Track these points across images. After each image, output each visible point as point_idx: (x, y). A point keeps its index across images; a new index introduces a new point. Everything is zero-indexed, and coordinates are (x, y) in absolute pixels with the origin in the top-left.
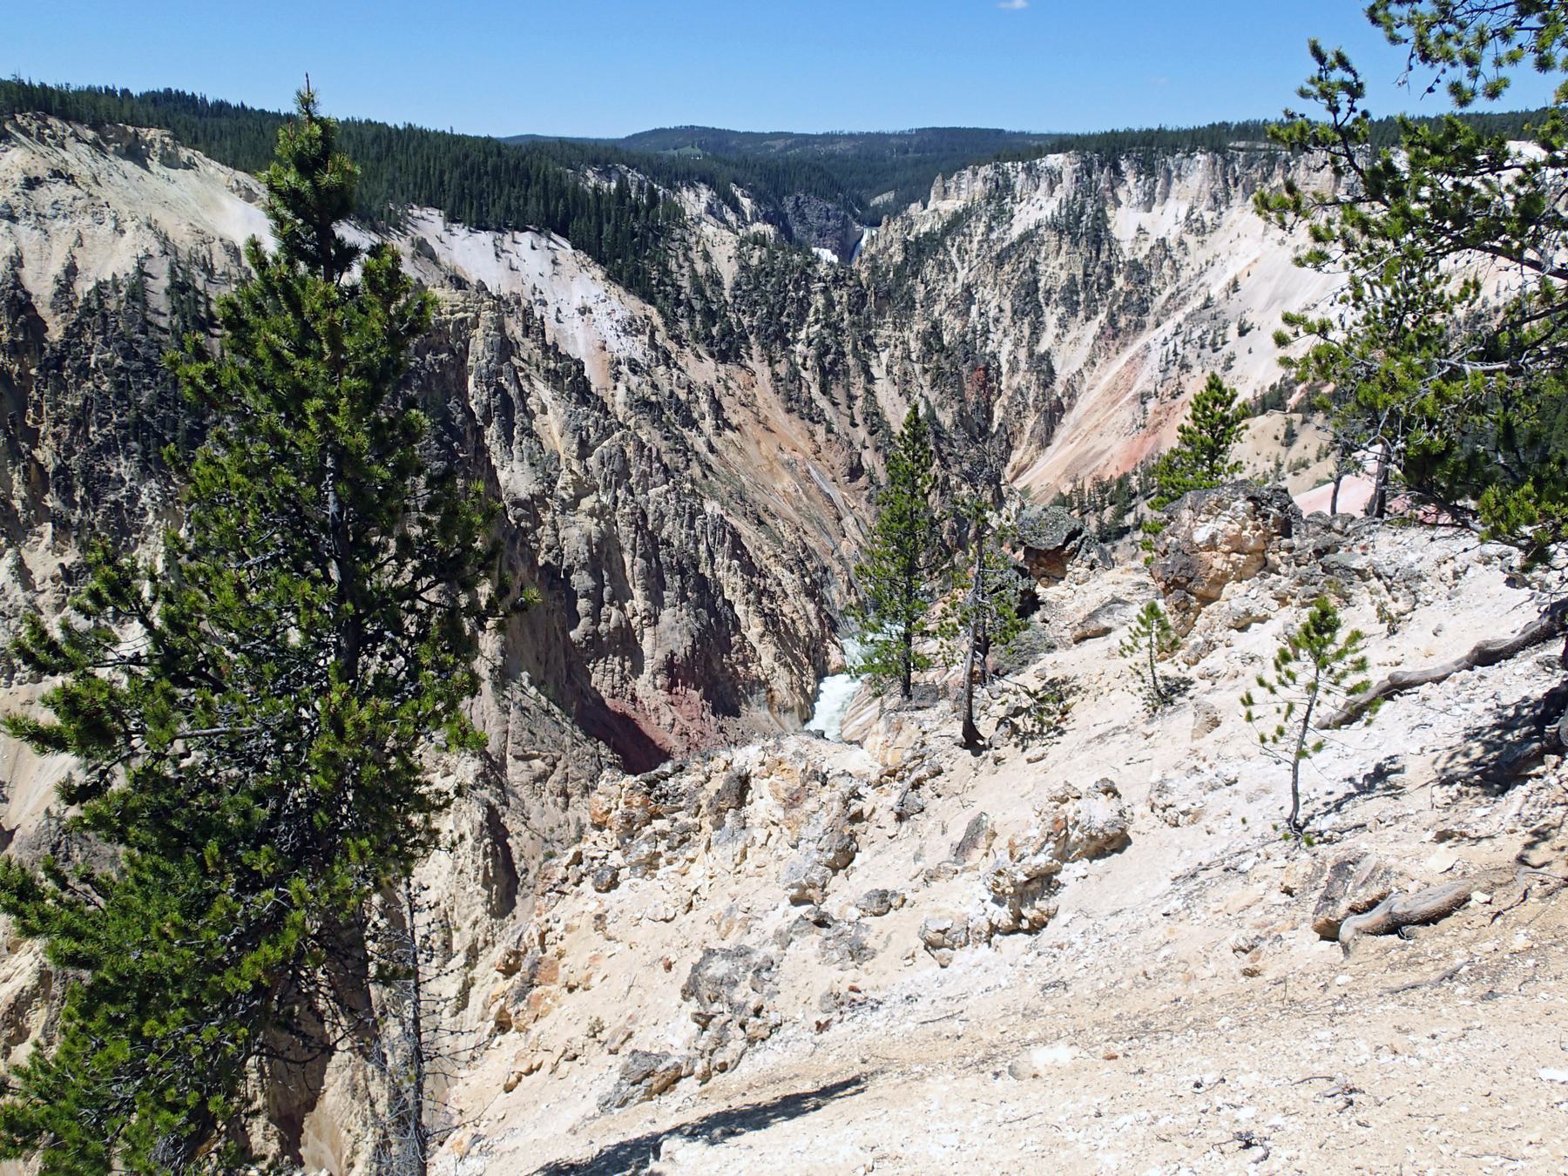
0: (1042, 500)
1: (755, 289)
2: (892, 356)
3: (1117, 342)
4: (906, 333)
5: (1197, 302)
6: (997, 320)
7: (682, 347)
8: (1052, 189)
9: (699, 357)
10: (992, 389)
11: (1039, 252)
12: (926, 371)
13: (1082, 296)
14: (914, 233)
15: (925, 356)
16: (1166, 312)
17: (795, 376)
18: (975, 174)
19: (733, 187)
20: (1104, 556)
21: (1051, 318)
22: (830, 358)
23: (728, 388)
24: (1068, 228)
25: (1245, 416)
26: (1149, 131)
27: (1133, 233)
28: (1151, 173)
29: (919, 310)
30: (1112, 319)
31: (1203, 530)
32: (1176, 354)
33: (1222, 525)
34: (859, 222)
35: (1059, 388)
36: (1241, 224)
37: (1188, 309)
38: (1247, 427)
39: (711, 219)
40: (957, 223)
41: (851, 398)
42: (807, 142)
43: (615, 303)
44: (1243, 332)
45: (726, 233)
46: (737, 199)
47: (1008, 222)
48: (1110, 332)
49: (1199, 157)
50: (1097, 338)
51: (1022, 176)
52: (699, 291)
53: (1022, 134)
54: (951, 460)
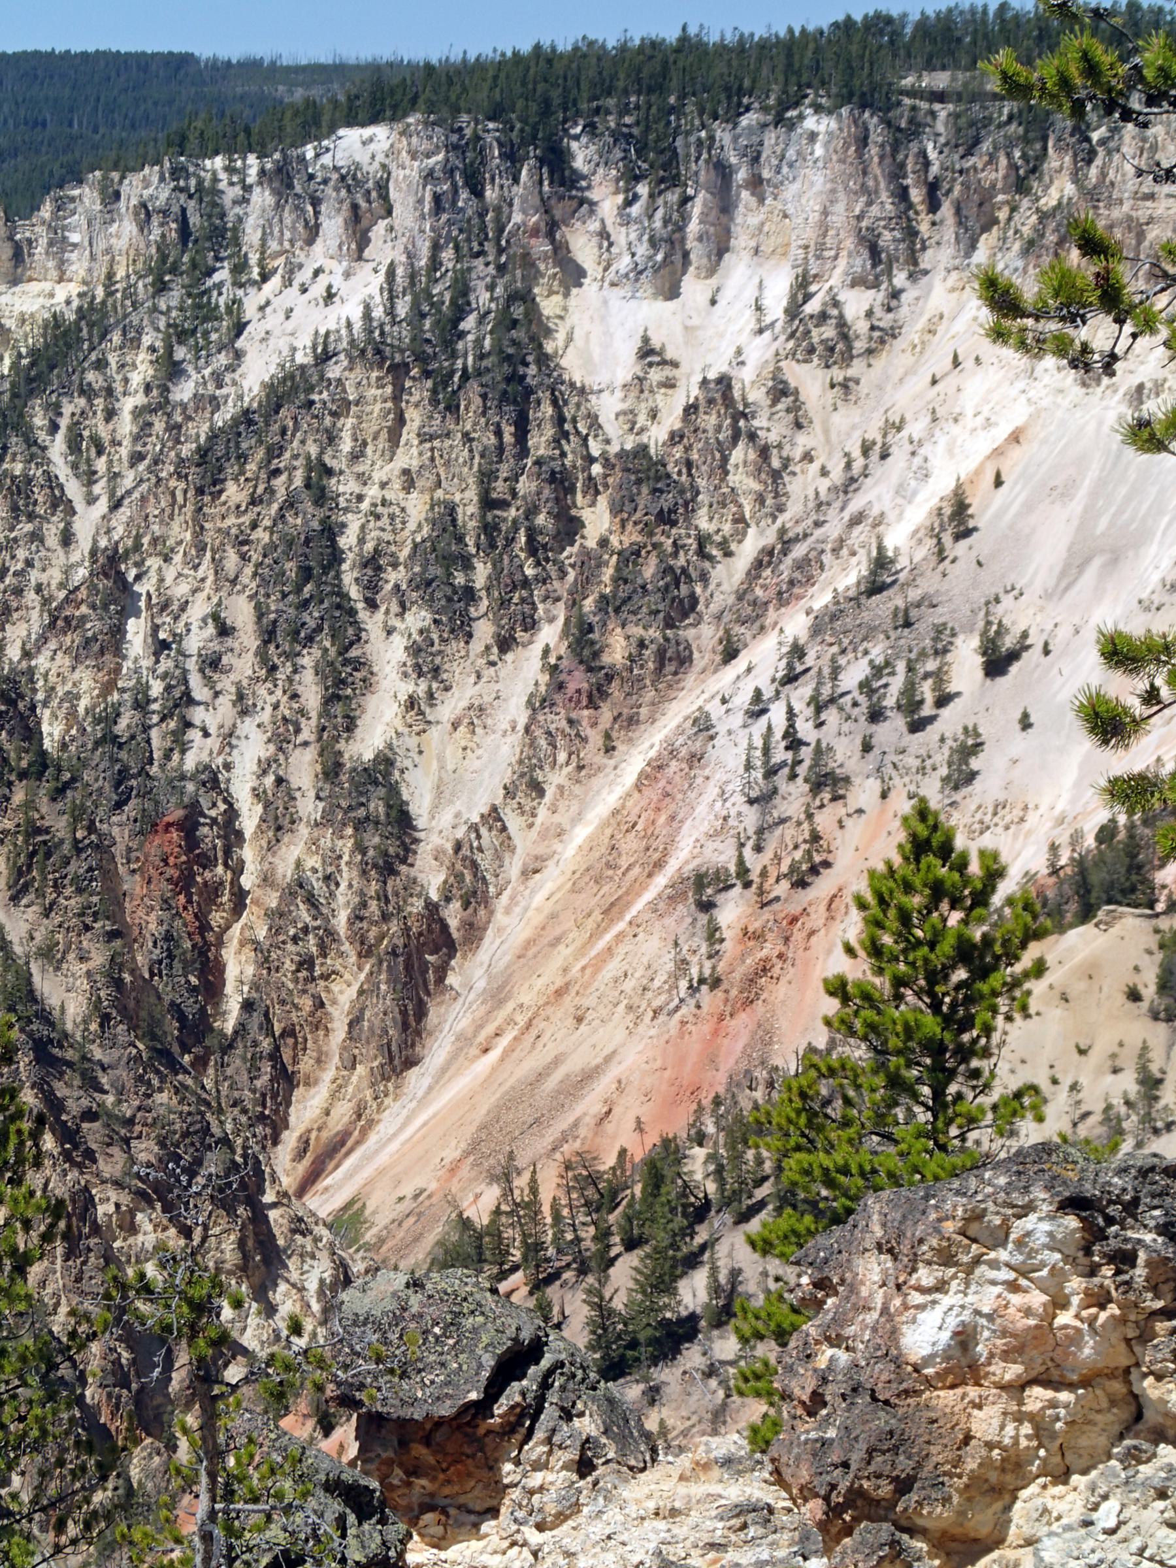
0: (403, 1249)
3: (606, 714)
5: (847, 575)
6: (212, 663)
10: (212, 891)
11: (332, 438)
13: (482, 572)
16: (752, 612)
20: (619, 1422)
21: (387, 651)
24: (421, 358)
25: (1032, 935)
26: (653, 47)
27: (625, 367)
28: (669, 176)
30: (584, 641)
31: (931, 1318)
33: (988, 1295)
35: (430, 875)
37: (820, 599)
38: (1039, 969)
44: (997, 663)
48: (579, 681)
49: (811, 123)
50: (539, 704)
51: (262, 198)
53: (251, 67)
54: (93, 1133)
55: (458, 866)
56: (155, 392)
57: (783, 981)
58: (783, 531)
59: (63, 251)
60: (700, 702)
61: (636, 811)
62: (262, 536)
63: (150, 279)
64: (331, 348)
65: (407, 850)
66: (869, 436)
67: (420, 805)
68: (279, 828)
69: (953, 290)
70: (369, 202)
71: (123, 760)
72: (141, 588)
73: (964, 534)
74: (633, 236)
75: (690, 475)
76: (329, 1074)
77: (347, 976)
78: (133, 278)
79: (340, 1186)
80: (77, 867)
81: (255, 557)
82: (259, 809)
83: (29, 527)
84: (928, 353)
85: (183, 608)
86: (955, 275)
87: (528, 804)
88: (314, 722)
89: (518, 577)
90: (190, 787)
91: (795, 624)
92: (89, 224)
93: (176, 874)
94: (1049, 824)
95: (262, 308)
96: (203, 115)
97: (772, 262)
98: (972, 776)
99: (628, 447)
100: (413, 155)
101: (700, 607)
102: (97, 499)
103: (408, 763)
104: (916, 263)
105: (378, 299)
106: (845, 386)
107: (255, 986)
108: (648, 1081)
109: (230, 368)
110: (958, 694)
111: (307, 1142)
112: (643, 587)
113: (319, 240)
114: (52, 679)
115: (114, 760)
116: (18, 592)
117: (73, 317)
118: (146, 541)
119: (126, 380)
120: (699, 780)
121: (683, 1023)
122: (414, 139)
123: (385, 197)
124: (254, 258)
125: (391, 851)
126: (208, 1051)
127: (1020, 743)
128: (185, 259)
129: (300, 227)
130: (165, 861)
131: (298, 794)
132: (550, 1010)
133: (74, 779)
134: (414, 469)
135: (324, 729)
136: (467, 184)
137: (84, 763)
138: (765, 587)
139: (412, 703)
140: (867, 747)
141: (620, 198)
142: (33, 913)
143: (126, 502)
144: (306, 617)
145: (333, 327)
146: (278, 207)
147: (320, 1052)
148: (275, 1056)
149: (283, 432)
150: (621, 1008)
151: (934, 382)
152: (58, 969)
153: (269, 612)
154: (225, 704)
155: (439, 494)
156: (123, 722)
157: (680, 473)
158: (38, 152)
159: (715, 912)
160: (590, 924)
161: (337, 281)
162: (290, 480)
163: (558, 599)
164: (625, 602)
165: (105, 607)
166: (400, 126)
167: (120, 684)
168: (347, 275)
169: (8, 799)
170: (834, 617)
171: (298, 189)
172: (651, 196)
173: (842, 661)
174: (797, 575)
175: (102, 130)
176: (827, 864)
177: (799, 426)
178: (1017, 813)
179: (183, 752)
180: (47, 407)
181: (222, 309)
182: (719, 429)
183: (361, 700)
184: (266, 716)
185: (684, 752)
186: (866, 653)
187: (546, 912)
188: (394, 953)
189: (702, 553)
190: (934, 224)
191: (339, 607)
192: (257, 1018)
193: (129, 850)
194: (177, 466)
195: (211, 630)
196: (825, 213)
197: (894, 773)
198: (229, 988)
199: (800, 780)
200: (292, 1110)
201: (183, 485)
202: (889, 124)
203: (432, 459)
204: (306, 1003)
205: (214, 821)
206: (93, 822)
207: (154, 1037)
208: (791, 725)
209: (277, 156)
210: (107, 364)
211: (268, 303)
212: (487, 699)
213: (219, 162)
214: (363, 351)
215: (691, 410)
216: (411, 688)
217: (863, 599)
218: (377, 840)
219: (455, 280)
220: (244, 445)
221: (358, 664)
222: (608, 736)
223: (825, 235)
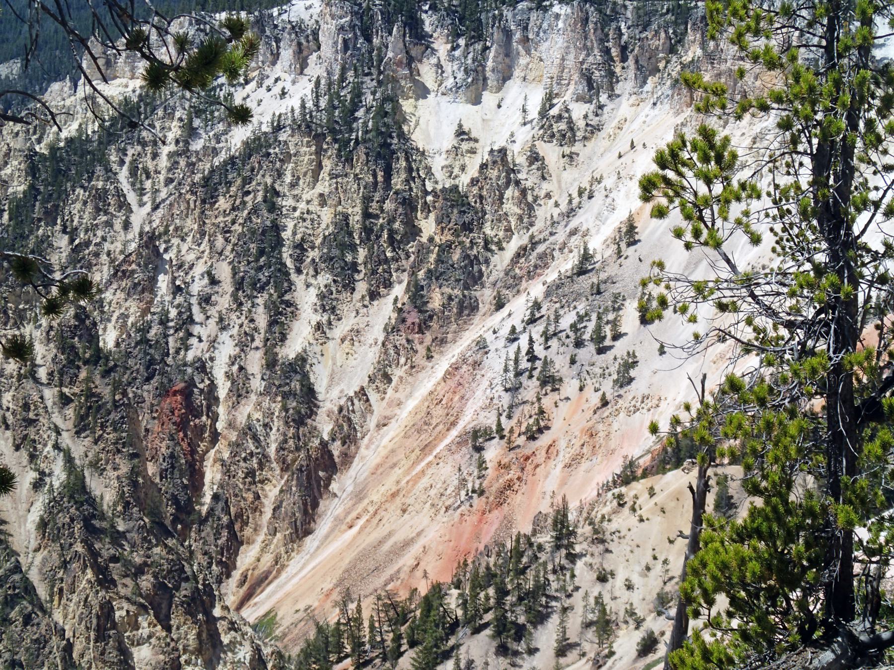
3: (428, 337)
5: (566, 264)
6: (206, 300)
8: (302, 64)
11: (280, 174)
12: (65, 401)
13: (362, 253)
14: (49, 138)
16: (513, 282)
21: (306, 297)
24: (333, 131)
27: (448, 140)
28: (477, 34)
30: (417, 294)
32: (533, 358)
35: (325, 426)
36: (636, 125)
37: (551, 276)
40: (129, 120)
48: (413, 318)
50: (391, 330)
55: (340, 421)
56: (181, 144)
57: (520, 493)
58: (532, 237)
60: (481, 332)
61: (442, 393)
62: (237, 228)
66: (583, 186)
67: (320, 387)
68: (239, 396)
69: (633, 105)
70: (308, 41)
71: (150, 353)
72: (166, 257)
73: (632, 243)
74: (455, 67)
75: (481, 203)
76: (260, 538)
77: (274, 482)
79: (263, 602)
81: (234, 240)
82: (229, 384)
83: (104, 218)
84: (617, 140)
85: (191, 267)
86: (634, 97)
87: (382, 386)
88: (262, 336)
89: (382, 257)
90: (189, 370)
91: (536, 290)
94: (673, 409)
97: (533, 85)
98: (631, 380)
99: (447, 186)
100: (333, 17)
101: (485, 278)
102: (145, 204)
104: (613, 90)
105: (310, 97)
106: (571, 157)
107: (221, 486)
108: (440, 548)
110: (626, 334)
111: (246, 577)
112: (452, 266)
114: (114, 305)
116: (97, 255)
118: (171, 228)
120: (478, 377)
121: (462, 515)
122: (334, 8)
123: (316, 39)
127: (659, 362)
132: (387, 505)
136: (363, 35)
137: (128, 355)
138: (521, 268)
139: (318, 327)
140: (573, 362)
141: (449, 46)
144: (261, 277)
145: (284, 111)
147: (256, 525)
148: (230, 526)
149: (253, 170)
150: (428, 505)
151: (620, 157)
154: (212, 322)
155: (340, 208)
156: (153, 332)
157: (476, 202)
159: (483, 452)
160: (413, 456)
161: (288, 86)
162: (255, 197)
163: (404, 271)
164: (441, 274)
165: (146, 266)
167: (152, 310)
168: (294, 82)
170: (558, 287)
171: (268, 33)
172: (467, 45)
173: (561, 312)
174: (539, 262)
176: (548, 428)
177: (544, 178)
178: (655, 402)
179: (187, 349)
180: (118, 150)
182: (498, 178)
184: (235, 331)
185: (471, 360)
186: (575, 308)
187: (389, 448)
188: (300, 470)
189: (486, 247)
190: (623, 68)
191: (279, 270)
192: (221, 504)
193: (152, 405)
195: (206, 281)
196: (563, 59)
197: (587, 377)
198: (206, 488)
199: (534, 379)
200: (239, 558)
201: (194, 198)
202: (600, 11)
203: (337, 189)
204: (250, 496)
205: (202, 391)
208: (531, 348)
209: (256, 13)
211: (248, 96)
212: (362, 326)
214: (299, 126)
215: (484, 166)
216: (319, 318)
217: (575, 277)
218: (295, 404)
219: (354, 88)
220: (230, 177)
221: (289, 304)
222: (429, 349)
223: (562, 72)
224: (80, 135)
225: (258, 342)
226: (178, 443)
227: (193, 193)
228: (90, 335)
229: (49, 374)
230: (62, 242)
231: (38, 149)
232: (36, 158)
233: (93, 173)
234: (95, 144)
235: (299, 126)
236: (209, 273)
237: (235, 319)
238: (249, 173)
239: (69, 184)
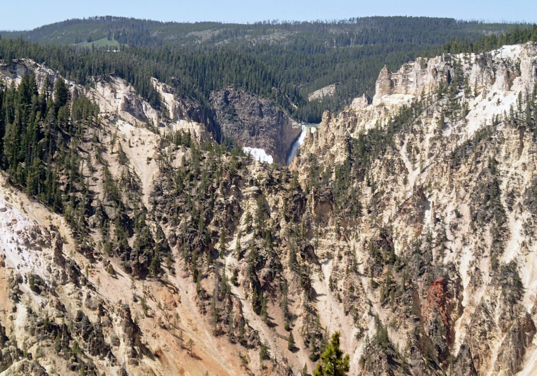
1: (178, 194)
2: (336, 268)
4: (352, 242)
6: (454, 227)
7: (93, 261)
9: (113, 272)
10: (452, 307)
11: (498, 151)
14: (358, 130)
15: (374, 269)
17: (224, 293)
18: (424, 66)
19: (154, 82)
22: (264, 272)
23: (146, 308)
24: (530, 125)
29: (366, 216)
34: (296, 118)
39: (129, 117)
40: (405, 119)
41: (290, 317)
42: (237, 33)
43: (17, 212)
45: (145, 132)
46: (158, 95)
47: (463, 118)
51: (476, 68)
52: (115, 197)
53: (474, 24)
56: (437, 133)
59: (407, 84)
62: (473, 184)
63: (437, 94)
64: (499, 120)
65: (520, 295)
67: (525, 279)
68: (476, 285)
77: (498, 338)
78: (431, 94)
80: (405, 295)
82: (469, 278)
83: (392, 177)
85: (445, 207)
88: (489, 249)
90: (445, 270)
92: (417, 75)
93: (439, 299)
95: (475, 106)
96: (456, 40)
100: (529, 55)
103: (522, 265)
105: (515, 104)
107: (466, 340)
109: (464, 126)
113: (495, 83)
114: (399, 230)
115: (419, 259)
116: (388, 199)
117: (410, 106)
118: (433, 184)
119: (428, 128)
122: (529, 50)
123: (518, 69)
124: (473, 89)
125: (515, 295)
126: (448, 362)
128: (449, 88)
129: (489, 78)
130: (436, 295)
131: (483, 274)
133: (405, 265)
134: (527, 163)
135: (492, 252)
137: (409, 259)
139: (524, 244)
142: (389, 311)
143: (426, 170)
144: (487, 212)
145: (499, 113)
146: (482, 71)
147: (487, 365)
148: (472, 365)
149: (481, 148)
152: (397, 331)
153: (475, 210)
154: (459, 241)
158: (400, 50)
161: (502, 98)
162: (483, 165)
165: (418, 206)
166: (524, 45)
167: (422, 233)
168: (505, 95)
169: (382, 271)
171: (489, 65)
175: (422, 43)
179: (443, 257)
181: (461, 105)
183: (506, 242)
184: (472, 246)
188: (515, 331)
192: (466, 352)
193: (423, 290)
194: (444, 158)
195: (454, 215)
198: (457, 340)
203: (533, 160)
204: (483, 347)
205: (453, 282)
206: (411, 280)
207: (429, 356)
209: (482, 54)
210: (421, 123)
211: (477, 104)
213: (461, 55)
214: (510, 122)
218: (510, 291)
220: (468, 152)
221: (505, 230)
224: (377, 128)
225: (487, 253)
226: (440, 314)
227: (445, 162)
228: (389, 246)
229: (365, 270)
230: (367, 191)
231: (352, 135)
232: (351, 141)
233: (385, 150)
234: (386, 133)
235: (510, 122)
236: (456, 211)
237: (473, 239)
238: (479, 150)
239: (371, 157)
